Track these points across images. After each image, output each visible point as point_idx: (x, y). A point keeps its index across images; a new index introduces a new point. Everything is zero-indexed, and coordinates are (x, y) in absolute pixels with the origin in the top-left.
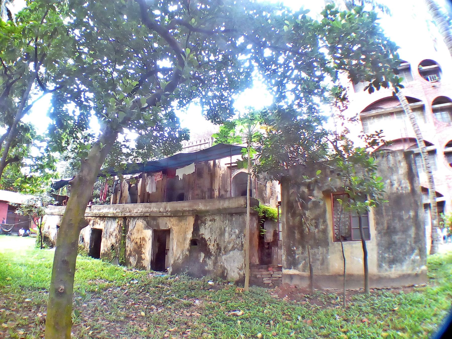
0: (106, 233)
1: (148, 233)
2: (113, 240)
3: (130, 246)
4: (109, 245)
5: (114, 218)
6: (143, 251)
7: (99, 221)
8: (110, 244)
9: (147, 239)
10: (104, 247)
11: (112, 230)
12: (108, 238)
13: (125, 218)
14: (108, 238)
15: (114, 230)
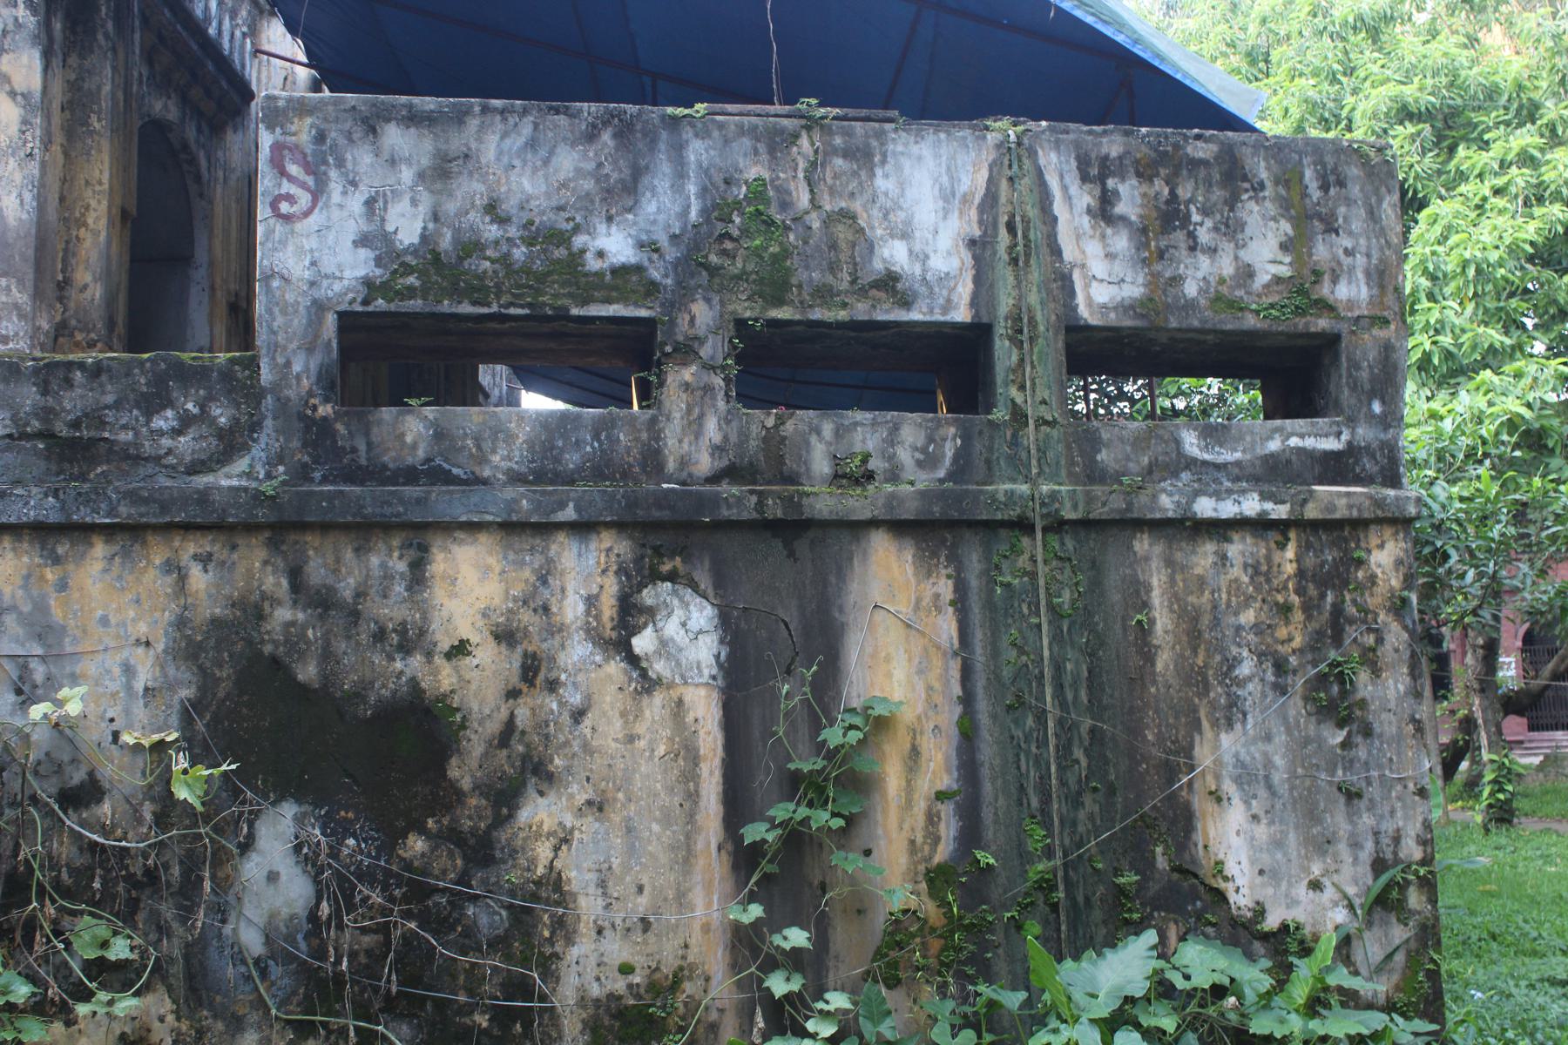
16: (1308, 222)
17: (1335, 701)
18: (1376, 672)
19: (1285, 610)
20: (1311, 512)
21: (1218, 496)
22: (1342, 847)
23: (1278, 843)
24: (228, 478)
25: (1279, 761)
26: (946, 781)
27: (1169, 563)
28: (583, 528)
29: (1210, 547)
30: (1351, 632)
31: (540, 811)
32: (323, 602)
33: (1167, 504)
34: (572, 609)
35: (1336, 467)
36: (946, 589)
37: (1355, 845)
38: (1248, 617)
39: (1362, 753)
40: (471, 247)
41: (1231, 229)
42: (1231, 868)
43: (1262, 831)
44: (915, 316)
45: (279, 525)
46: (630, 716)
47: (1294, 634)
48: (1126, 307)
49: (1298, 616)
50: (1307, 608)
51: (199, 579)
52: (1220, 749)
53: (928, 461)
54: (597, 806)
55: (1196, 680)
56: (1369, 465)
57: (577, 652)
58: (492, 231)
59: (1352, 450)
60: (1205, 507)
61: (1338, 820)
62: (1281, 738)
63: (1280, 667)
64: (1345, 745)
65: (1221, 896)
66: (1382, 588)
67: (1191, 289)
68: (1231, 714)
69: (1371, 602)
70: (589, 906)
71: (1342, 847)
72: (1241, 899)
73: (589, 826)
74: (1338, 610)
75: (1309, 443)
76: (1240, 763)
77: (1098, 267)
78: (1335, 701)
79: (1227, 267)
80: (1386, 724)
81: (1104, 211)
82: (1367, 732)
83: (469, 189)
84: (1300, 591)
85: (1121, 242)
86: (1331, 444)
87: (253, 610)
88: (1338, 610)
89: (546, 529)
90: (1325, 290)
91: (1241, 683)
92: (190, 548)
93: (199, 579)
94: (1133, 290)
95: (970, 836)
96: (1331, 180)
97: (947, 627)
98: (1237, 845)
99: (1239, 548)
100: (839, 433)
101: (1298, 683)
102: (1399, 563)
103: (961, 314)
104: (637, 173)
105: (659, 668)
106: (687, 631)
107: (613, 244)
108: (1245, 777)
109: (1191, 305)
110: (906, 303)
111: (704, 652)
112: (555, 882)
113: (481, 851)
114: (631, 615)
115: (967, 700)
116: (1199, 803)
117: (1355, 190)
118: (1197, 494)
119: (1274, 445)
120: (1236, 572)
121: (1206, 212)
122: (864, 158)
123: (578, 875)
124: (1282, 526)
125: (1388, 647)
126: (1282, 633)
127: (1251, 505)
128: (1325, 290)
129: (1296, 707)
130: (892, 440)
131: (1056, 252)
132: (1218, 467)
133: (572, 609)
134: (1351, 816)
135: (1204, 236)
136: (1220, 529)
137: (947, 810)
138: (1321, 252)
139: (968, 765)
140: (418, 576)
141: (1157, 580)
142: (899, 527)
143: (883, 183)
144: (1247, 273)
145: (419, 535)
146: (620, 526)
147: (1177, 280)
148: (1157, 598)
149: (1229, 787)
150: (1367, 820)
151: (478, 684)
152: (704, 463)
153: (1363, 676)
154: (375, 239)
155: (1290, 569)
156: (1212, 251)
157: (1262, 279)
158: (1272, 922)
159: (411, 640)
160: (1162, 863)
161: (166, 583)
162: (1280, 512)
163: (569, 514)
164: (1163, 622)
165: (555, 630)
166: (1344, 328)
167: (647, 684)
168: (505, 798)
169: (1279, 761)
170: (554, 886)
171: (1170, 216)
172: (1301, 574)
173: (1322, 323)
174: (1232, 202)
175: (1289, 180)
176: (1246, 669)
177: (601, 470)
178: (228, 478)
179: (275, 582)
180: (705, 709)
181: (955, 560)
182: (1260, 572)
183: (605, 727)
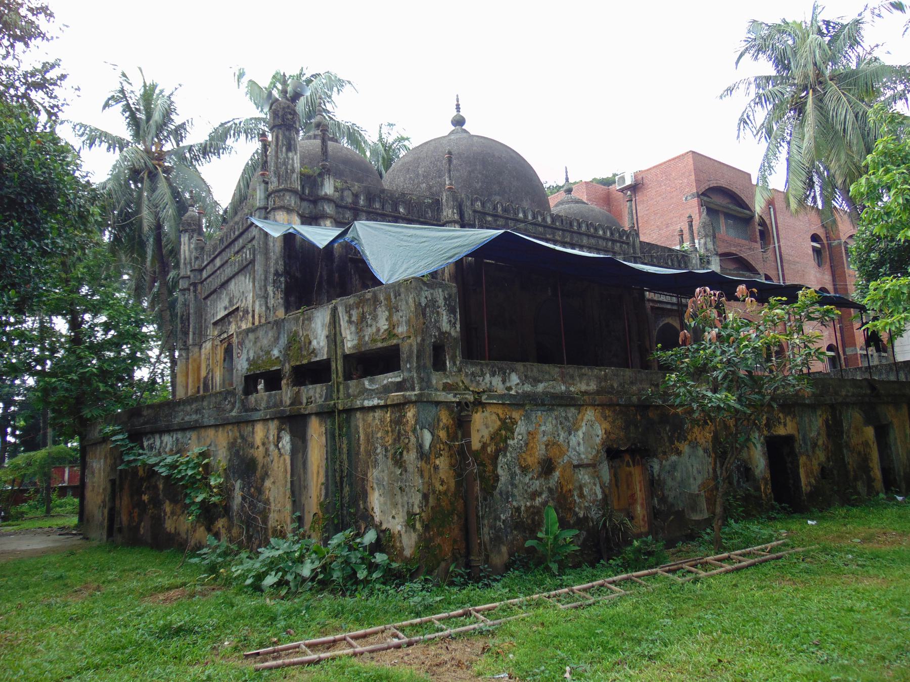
0: (805, 444)
1: (870, 432)
2: (821, 456)
3: (851, 460)
4: (816, 468)
5: (813, 407)
6: (871, 465)
7: (781, 415)
8: (817, 466)
9: (871, 443)
10: (807, 476)
11: (813, 434)
12: (810, 453)
13: (832, 407)
14: (810, 453)
15: (819, 434)
16: (393, 309)
17: (399, 461)
18: (408, 452)
19: (387, 432)
20: (389, 403)
21: (368, 399)
22: (400, 506)
23: (385, 503)
24: (233, 414)
25: (386, 479)
26: (323, 480)
27: (363, 420)
28: (272, 419)
29: (371, 414)
30: (402, 438)
31: (268, 483)
32: (242, 437)
33: (358, 403)
34: (271, 438)
35: (399, 387)
36: (323, 429)
37: (403, 506)
38: (379, 435)
39: (404, 477)
40: (259, 357)
41: (375, 318)
42: (375, 510)
43: (382, 499)
44: (318, 359)
45: (238, 422)
46: (279, 462)
47: (389, 440)
48: (354, 347)
49: (390, 434)
50: (392, 431)
51: (230, 434)
52: (374, 474)
53: (321, 397)
54: (274, 483)
55: (368, 454)
56: (408, 385)
57: (272, 447)
58: (261, 353)
59: (404, 380)
60: (367, 403)
61: (399, 498)
62: (386, 472)
63: (386, 450)
64: (401, 474)
65: (373, 517)
66: (409, 425)
67: (367, 338)
68: (375, 464)
69: (407, 429)
70: (273, 507)
71: (400, 506)
72: (377, 519)
73: (273, 487)
74: (399, 432)
75: (393, 380)
76: (378, 479)
77: (349, 338)
78: (399, 461)
79: (374, 330)
80: (411, 468)
81: (350, 322)
82: (406, 471)
83: (259, 344)
84: (391, 426)
85: (353, 329)
86: (399, 379)
87: (235, 440)
88: (399, 432)
89: (268, 420)
90: (396, 331)
91: (378, 455)
92: (230, 427)
93: (230, 434)
94: (355, 342)
95: (326, 495)
96: (397, 294)
97: (324, 439)
98: (376, 501)
99: (378, 414)
100: (308, 391)
101: (390, 454)
102: (414, 416)
103: (325, 357)
104: (279, 334)
105: (282, 451)
106: (286, 441)
107: (276, 353)
108: (380, 483)
109: (367, 343)
110: (316, 356)
111: (288, 447)
112: (268, 499)
113: (260, 490)
114: (279, 439)
115: (327, 459)
116: (369, 489)
117: (403, 296)
118: (364, 399)
119: (385, 382)
120: (377, 421)
121: (370, 314)
122: (310, 319)
123: (272, 499)
124: (385, 407)
125: (411, 443)
126: (387, 439)
127: (375, 402)
128: (396, 331)
129: (390, 462)
130: (315, 392)
131: (341, 335)
132: (373, 390)
133: (271, 438)
134: (402, 496)
135: (369, 322)
136: (373, 408)
137: (323, 487)
138: (395, 318)
139: (327, 476)
140: (253, 433)
141: (361, 424)
142: (317, 414)
143: (313, 325)
144: (378, 330)
145: (253, 422)
146: (278, 418)
147: (364, 336)
148: (361, 430)
149: (375, 486)
150: (406, 498)
151: (259, 453)
152: (288, 402)
153: (405, 453)
154: (248, 360)
155: (388, 419)
156: (371, 326)
157: (382, 331)
158: (384, 527)
159: (252, 445)
160: (362, 506)
161: (226, 434)
162: (382, 403)
163: (268, 417)
164: (362, 437)
165: (269, 443)
166: (400, 341)
167: (281, 455)
168: (263, 480)
169: (386, 479)
170: (267, 502)
171: (363, 318)
172: (391, 421)
173: (395, 342)
174: (375, 309)
175: (388, 299)
176: (378, 451)
177: (275, 405)
178: (233, 414)
179: (238, 434)
180: (288, 462)
181: (325, 422)
182: (382, 421)
183: (275, 464)
